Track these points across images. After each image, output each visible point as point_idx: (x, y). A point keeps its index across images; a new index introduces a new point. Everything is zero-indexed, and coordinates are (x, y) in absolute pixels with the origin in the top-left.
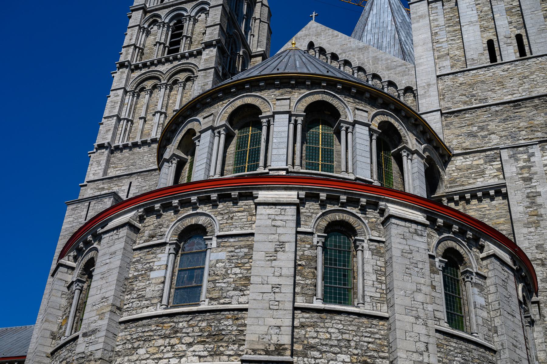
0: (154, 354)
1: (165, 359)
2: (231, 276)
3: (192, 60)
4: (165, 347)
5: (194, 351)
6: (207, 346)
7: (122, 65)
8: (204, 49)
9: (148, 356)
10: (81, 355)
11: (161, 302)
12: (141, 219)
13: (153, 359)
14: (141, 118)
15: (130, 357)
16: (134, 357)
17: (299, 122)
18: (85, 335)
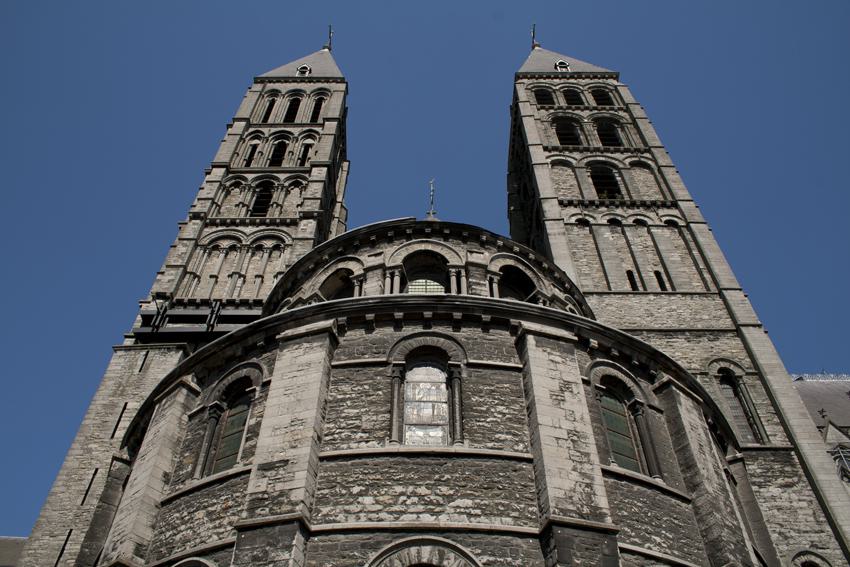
0: (390, 505)
1: (412, 513)
2: (496, 414)
4: (409, 497)
5: (458, 507)
6: (478, 501)
7: (196, 216)
8: (301, 219)
9: (379, 507)
10: (260, 496)
11: (390, 436)
12: (342, 330)
13: (391, 513)
14: (211, 276)
15: (347, 507)
16: (353, 508)
18: (265, 468)
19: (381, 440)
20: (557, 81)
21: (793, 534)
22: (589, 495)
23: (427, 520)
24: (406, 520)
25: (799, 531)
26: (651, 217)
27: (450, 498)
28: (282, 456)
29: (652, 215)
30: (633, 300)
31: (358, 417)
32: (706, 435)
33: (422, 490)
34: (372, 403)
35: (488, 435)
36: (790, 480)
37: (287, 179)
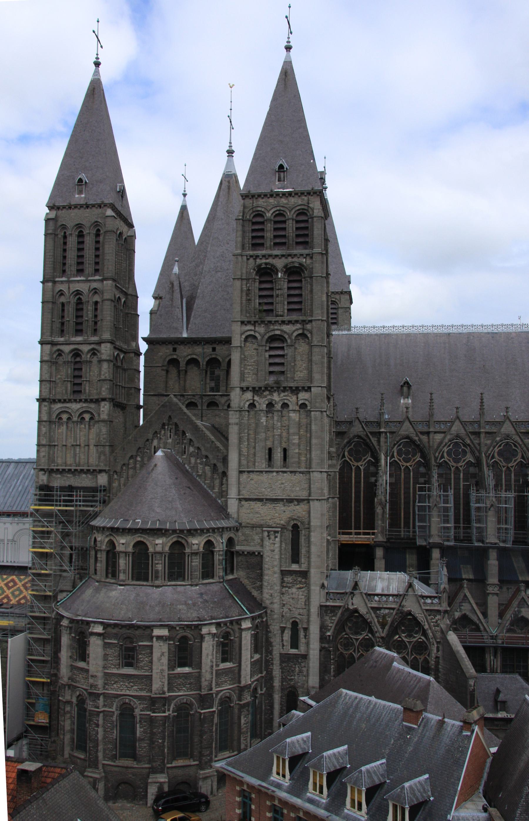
3: (93, 406)
17: (167, 556)
19: (117, 668)
20: (271, 200)
21: (294, 609)
22: (163, 688)
23: (128, 692)
24: (123, 693)
25: (297, 608)
26: (292, 400)
27: (132, 686)
28: (95, 674)
29: (294, 398)
30: (264, 477)
31: (112, 661)
32: (213, 647)
33: (127, 684)
34: (115, 656)
35: (142, 668)
36: (301, 586)
37: (89, 351)
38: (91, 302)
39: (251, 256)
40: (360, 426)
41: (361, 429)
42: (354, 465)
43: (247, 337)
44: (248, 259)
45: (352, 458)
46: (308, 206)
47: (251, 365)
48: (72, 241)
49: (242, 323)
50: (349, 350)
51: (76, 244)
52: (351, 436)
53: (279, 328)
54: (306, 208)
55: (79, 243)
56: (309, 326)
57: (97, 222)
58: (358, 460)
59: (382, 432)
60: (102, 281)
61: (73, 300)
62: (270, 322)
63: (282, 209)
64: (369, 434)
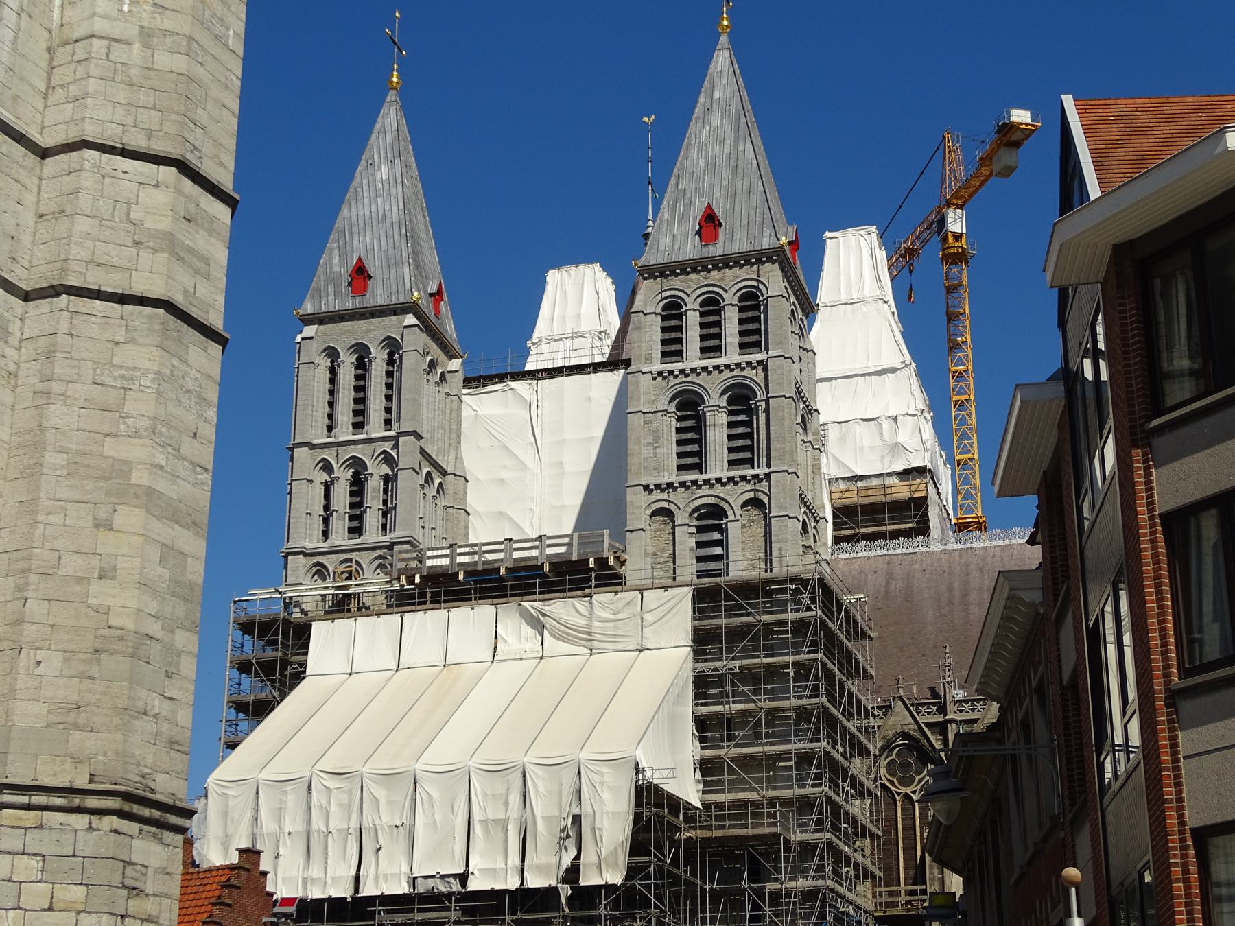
38: (376, 477)
39: (660, 374)
40: (907, 713)
41: (910, 720)
42: (899, 794)
43: (654, 514)
44: (654, 379)
45: (895, 780)
46: (759, 281)
47: (665, 562)
48: (347, 374)
49: (646, 487)
50: (888, 583)
51: (353, 379)
52: (891, 733)
53: (711, 492)
54: (755, 284)
55: (357, 377)
56: (764, 486)
57: (388, 338)
58: (906, 782)
59: (951, 721)
60: (396, 438)
61: (344, 476)
62: (695, 483)
63: (711, 289)
64: (926, 729)
